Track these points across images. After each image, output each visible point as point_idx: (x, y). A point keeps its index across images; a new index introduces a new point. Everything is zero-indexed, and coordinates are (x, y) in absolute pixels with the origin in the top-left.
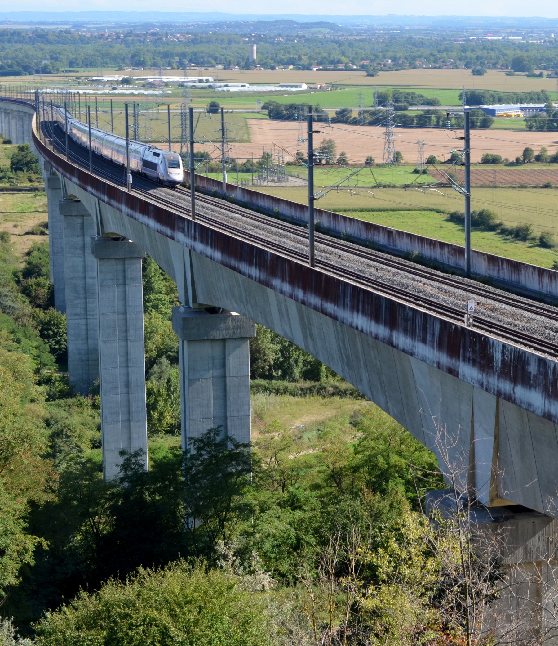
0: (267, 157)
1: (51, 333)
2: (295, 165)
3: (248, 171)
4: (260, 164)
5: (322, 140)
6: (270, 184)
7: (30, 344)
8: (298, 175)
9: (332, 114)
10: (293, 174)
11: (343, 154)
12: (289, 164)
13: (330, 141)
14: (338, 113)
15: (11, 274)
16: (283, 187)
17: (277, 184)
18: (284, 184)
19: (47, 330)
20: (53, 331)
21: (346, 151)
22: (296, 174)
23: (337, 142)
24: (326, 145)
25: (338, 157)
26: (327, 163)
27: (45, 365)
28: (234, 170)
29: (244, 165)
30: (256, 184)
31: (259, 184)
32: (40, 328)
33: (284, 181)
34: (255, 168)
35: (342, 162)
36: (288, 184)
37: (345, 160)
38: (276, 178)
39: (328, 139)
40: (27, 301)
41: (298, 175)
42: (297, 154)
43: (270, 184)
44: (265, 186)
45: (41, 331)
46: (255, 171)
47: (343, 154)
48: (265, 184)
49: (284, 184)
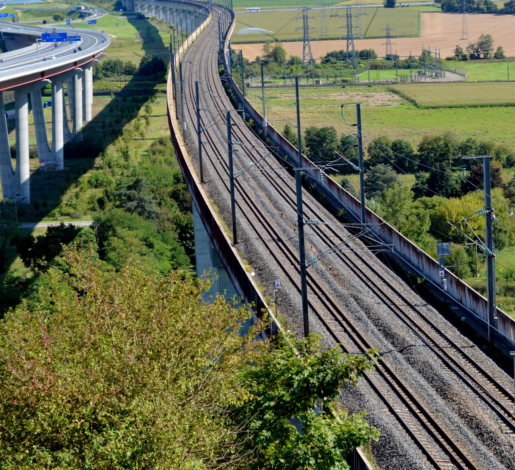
0: (426, 54)
1: (188, 235)
2: (454, 59)
3: (409, 67)
4: (422, 59)
5: (480, 35)
6: (428, 80)
7: (166, 246)
8: (455, 70)
9: (501, 6)
10: (451, 69)
11: (500, 49)
12: (449, 59)
13: (488, 36)
14: (506, 5)
15: (172, 176)
16: (439, 82)
17: (433, 80)
18: (440, 80)
19: (185, 233)
20: (190, 234)
21: (502, 46)
22: (453, 69)
23: (494, 37)
24: (484, 40)
25: (495, 51)
26: (485, 58)
27: (180, 265)
28: (396, 66)
29: (406, 61)
30: (414, 80)
31: (417, 80)
32: (179, 231)
33: (441, 76)
34: (416, 64)
35: (499, 56)
36: (444, 80)
37: (501, 54)
38: (434, 74)
39: (485, 34)
40: (176, 205)
41: (455, 70)
42: (457, 50)
43: (428, 80)
44: (423, 82)
45: (179, 234)
46: (416, 67)
47: (500, 49)
48: (423, 80)
49: (440, 80)
